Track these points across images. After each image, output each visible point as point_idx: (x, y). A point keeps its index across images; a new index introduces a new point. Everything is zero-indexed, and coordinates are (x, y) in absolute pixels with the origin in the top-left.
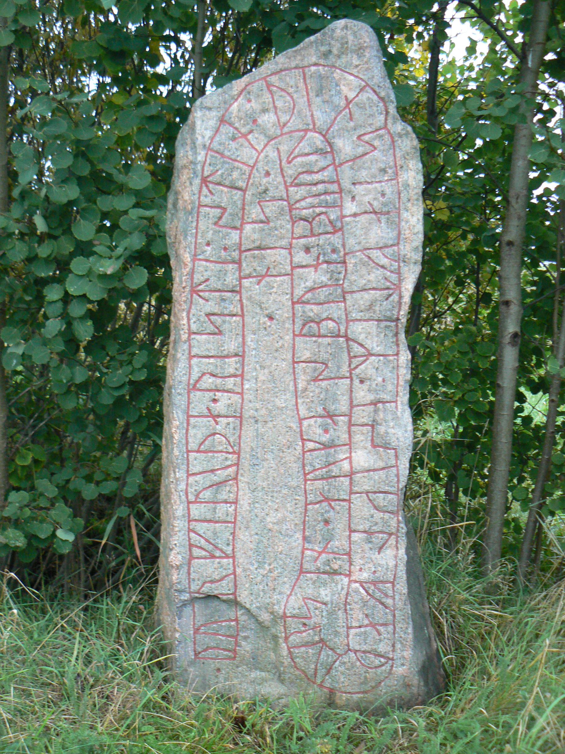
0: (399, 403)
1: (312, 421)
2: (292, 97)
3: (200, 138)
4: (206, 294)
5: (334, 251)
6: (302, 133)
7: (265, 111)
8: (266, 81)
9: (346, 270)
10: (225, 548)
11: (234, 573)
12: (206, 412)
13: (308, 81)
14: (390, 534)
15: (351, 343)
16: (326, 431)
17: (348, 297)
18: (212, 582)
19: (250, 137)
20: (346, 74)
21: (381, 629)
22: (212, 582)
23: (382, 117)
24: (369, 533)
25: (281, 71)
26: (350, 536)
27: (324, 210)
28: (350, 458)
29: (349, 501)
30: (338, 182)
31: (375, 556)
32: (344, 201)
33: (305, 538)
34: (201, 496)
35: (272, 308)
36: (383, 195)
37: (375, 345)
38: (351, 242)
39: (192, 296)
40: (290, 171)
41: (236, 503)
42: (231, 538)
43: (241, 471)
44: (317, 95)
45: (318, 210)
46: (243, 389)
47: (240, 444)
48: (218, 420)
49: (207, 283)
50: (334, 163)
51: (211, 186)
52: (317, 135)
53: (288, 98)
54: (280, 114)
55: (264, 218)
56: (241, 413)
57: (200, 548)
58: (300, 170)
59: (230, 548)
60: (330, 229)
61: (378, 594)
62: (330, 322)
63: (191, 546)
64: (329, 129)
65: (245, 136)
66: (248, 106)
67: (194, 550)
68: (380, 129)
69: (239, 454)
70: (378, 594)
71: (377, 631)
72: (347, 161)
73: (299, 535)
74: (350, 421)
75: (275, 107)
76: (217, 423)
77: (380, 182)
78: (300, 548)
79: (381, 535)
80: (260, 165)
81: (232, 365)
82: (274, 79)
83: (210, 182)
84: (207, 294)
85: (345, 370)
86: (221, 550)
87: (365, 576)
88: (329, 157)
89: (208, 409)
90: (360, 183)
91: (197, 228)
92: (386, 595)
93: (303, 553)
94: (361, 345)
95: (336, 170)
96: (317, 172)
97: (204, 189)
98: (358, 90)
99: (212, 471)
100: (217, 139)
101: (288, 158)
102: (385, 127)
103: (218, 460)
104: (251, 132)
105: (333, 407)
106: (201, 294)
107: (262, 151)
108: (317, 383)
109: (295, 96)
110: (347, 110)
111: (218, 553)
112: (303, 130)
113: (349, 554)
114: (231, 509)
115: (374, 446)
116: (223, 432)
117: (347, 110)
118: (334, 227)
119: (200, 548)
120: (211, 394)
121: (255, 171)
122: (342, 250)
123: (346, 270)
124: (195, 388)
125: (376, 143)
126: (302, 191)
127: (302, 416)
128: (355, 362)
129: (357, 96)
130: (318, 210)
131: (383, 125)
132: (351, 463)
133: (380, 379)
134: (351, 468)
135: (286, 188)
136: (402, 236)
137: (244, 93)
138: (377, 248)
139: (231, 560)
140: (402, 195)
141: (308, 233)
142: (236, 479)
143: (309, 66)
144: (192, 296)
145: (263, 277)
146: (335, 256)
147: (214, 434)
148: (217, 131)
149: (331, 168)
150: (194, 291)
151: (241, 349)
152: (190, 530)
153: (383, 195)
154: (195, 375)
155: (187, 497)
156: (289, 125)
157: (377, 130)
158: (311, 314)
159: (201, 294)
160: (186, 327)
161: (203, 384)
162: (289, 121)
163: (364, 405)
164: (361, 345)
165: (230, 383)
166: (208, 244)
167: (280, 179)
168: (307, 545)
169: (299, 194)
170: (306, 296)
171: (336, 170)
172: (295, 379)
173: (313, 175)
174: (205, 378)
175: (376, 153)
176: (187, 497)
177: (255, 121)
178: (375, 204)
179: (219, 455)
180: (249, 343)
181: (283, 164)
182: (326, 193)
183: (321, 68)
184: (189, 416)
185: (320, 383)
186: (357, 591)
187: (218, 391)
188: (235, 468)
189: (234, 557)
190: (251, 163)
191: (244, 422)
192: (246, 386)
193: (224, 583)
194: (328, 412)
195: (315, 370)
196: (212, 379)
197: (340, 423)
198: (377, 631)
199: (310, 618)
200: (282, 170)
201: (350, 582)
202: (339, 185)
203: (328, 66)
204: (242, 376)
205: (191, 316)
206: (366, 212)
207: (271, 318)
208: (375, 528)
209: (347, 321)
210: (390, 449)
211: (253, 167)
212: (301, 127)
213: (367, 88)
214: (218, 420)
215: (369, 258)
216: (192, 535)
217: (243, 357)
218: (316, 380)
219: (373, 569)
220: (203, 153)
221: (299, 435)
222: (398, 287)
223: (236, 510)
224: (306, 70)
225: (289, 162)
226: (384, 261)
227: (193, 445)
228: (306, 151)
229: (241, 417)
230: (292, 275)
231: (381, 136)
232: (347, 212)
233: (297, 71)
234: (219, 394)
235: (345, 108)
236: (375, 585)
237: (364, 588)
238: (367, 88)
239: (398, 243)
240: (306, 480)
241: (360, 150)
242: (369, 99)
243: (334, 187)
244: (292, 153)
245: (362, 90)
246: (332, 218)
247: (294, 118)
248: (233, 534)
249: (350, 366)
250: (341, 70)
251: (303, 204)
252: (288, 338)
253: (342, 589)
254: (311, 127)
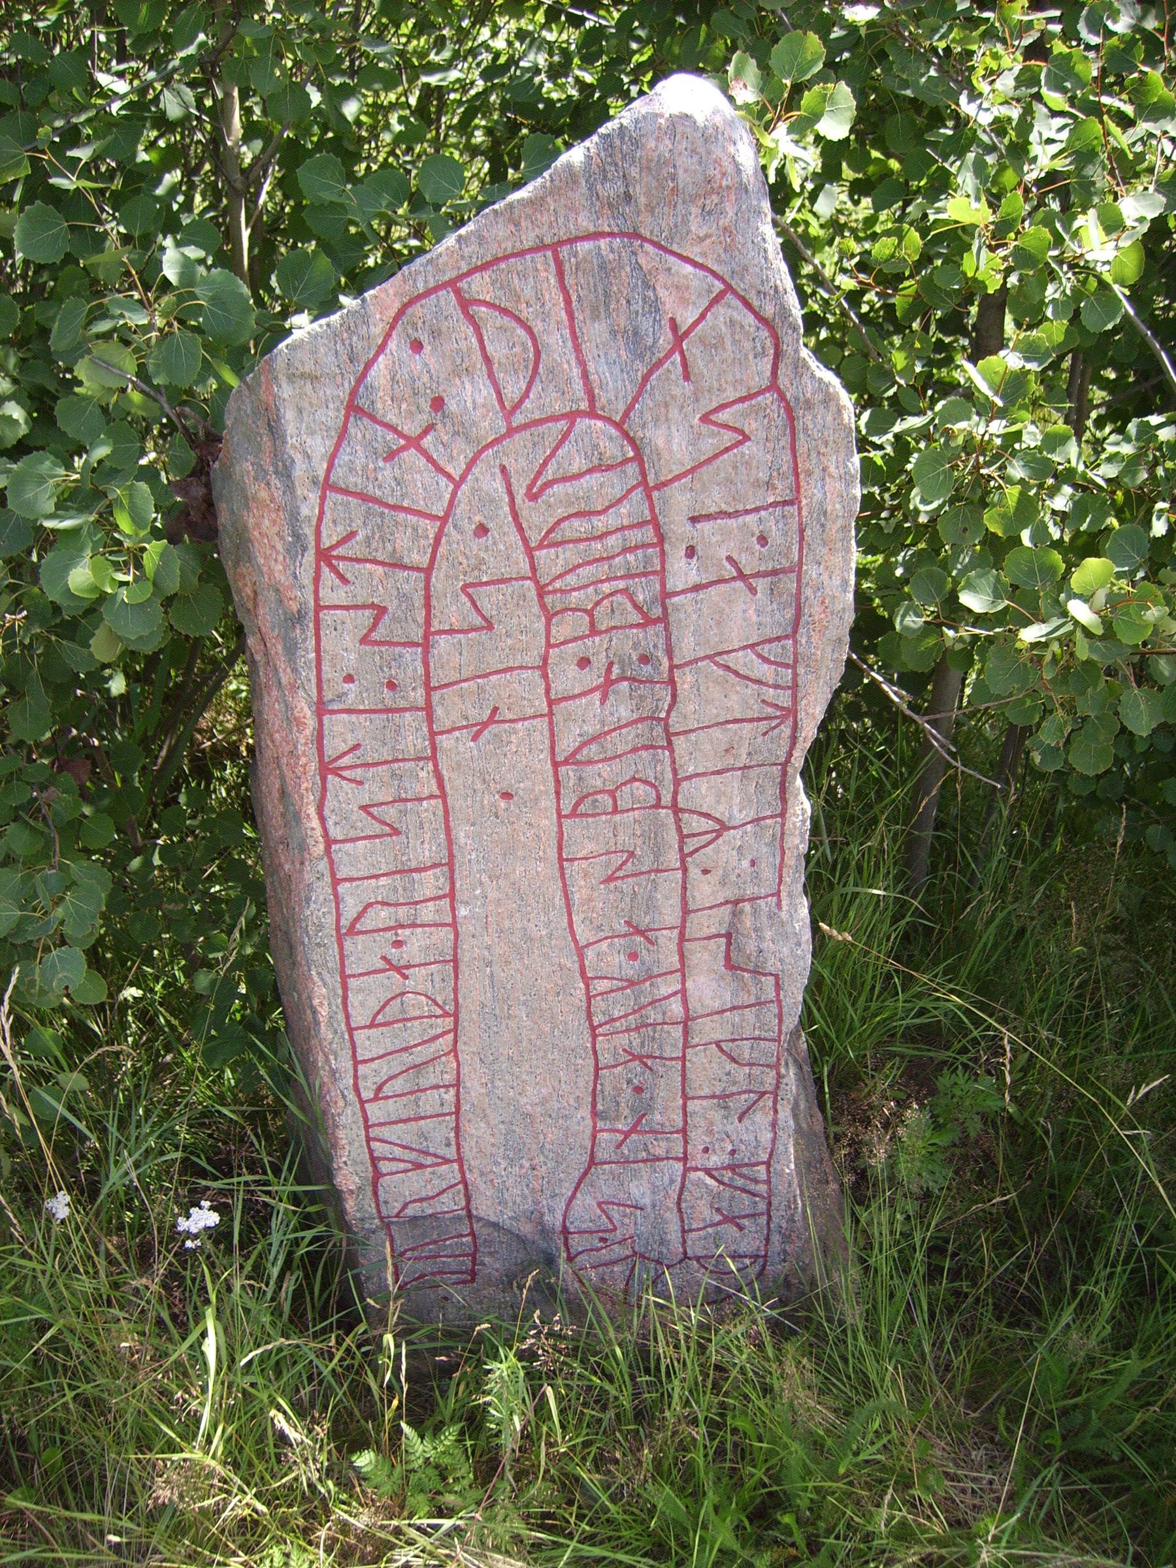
0: (783, 894)
1: (604, 946)
2: (529, 330)
3: (298, 458)
4: (358, 773)
5: (645, 659)
6: (563, 425)
7: (460, 371)
8: (458, 292)
9: (674, 696)
10: (440, 1152)
11: (464, 1181)
12: (381, 964)
13: (569, 281)
16: (633, 956)
17: (678, 742)
18: (421, 1200)
19: (428, 442)
20: (672, 259)
21: (745, 1222)
22: (421, 1200)
23: (766, 365)
24: (723, 1098)
25: (497, 260)
26: (684, 1106)
27: (621, 584)
28: (683, 992)
30: (655, 522)
31: (734, 1126)
32: (670, 560)
33: (595, 1114)
34: (385, 1089)
35: (509, 780)
36: (763, 540)
38: (687, 647)
39: (324, 780)
40: (537, 518)
41: (457, 1084)
42: (452, 1134)
44: (595, 317)
45: (606, 588)
46: (454, 916)
47: (456, 1000)
48: (406, 972)
49: (357, 752)
50: (644, 482)
52: (600, 424)
53: (520, 332)
55: (478, 621)
56: (455, 954)
58: (561, 512)
59: (454, 1148)
60: (636, 618)
61: (740, 1182)
62: (637, 784)
63: (374, 1160)
64: (630, 408)
65: (414, 442)
66: (416, 364)
68: (760, 393)
70: (740, 1182)
72: (678, 478)
73: (585, 1112)
75: (487, 360)
76: (406, 977)
77: (757, 510)
78: (588, 1132)
80: (461, 509)
82: (479, 286)
83: (339, 558)
84: (359, 771)
85: (672, 858)
86: (436, 1156)
87: (714, 1160)
89: (384, 958)
90: (709, 517)
92: (756, 1181)
93: (594, 1137)
94: (707, 816)
95: (649, 498)
99: (405, 1049)
100: (343, 457)
101: (530, 487)
102: (774, 386)
103: (415, 1032)
104: (429, 428)
106: (345, 773)
107: (463, 478)
108: (612, 885)
109: (538, 326)
110: (677, 357)
111: (429, 1160)
112: (563, 416)
113: (684, 1131)
115: (730, 965)
116: (420, 988)
118: (644, 615)
120: (389, 934)
121: (450, 528)
123: (674, 696)
124: (352, 931)
125: (751, 426)
129: (703, 316)
130: (606, 588)
131: (766, 383)
132: (685, 1002)
133: (745, 864)
135: (529, 551)
136: (804, 619)
137: (399, 327)
138: (744, 648)
139: (456, 1166)
140: (808, 532)
142: (455, 1050)
144: (324, 780)
145: (485, 725)
146: (647, 670)
147: (404, 994)
148: (343, 434)
149: (638, 495)
150: (327, 769)
151: (445, 852)
152: (369, 1139)
153: (763, 540)
154: (351, 909)
156: (527, 404)
157: (750, 397)
159: (345, 773)
160: (319, 831)
162: (526, 395)
163: (711, 908)
164: (707, 816)
166: (349, 679)
167: (514, 537)
168: (600, 1125)
169: (560, 562)
170: (585, 751)
171: (649, 498)
172: (565, 885)
173: (595, 520)
174: (371, 912)
175: (745, 448)
177: (438, 403)
178: (743, 560)
179: (416, 1023)
180: (462, 841)
182: (626, 550)
183: (603, 243)
184: (344, 978)
186: (699, 1183)
187: (402, 926)
189: (460, 1160)
191: (463, 967)
192: (463, 911)
193: (444, 1198)
195: (608, 864)
196: (384, 913)
199: (615, 1229)
201: (687, 1170)
202: (657, 527)
203: (622, 234)
204: (452, 895)
205: (326, 812)
207: (507, 796)
208: (734, 1089)
209: (677, 782)
210: (765, 975)
211: (444, 520)
212: (559, 407)
213: (729, 296)
214: (406, 972)
215: (727, 668)
217: (451, 864)
218: (610, 879)
219: (730, 1148)
220: (314, 497)
221: (577, 974)
222: (791, 713)
224: (564, 251)
225: (533, 497)
228: (575, 469)
229: (455, 961)
230: (551, 714)
231: (758, 411)
232: (675, 582)
233: (539, 257)
235: (668, 355)
237: (713, 1177)
238: (729, 296)
239: (795, 632)
240: (594, 1037)
241: (709, 445)
242: (732, 323)
243: (648, 534)
244: (539, 474)
247: (537, 387)
249: (681, 849)
251: (571, 580)
252: (548, 823)
253: (672, 1181)
254: (584, 406)
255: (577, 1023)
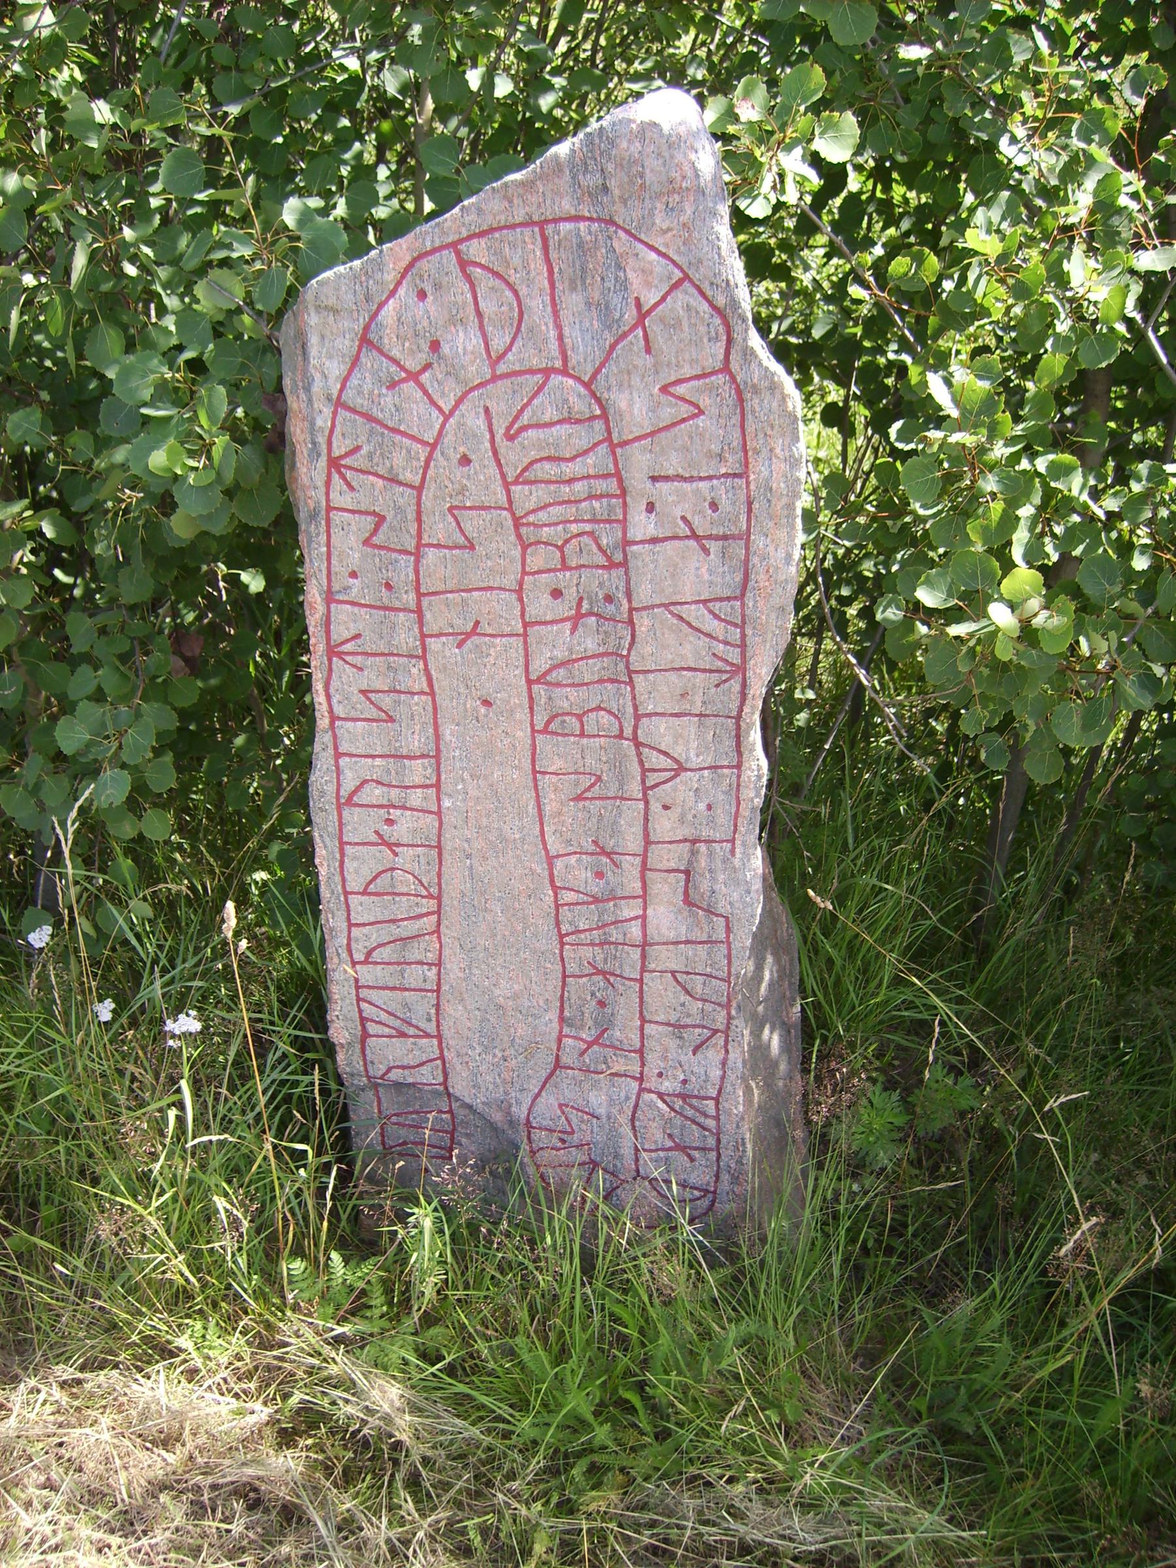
0: (738, 843)
1: (573, 860)
2: (516, 293)
3: (317, 376)
4: (358, 660)
5: (609, 599)
6: (539, 378)
7: (456, 321)
8: (458, 253)
9: (633, 636)
10: (422, 1025)
11: (442, 1058)
12: (374, 838)
13: (553, 255)
14: (716, 1031)
15: (646, 751)
16: (600, 875)
17: (638, 679)
18: (403, 1067)
19: (425, 378)
20: (640, 246)
21: (696, 1154)
22: (403, 1067)
23: (719, 349)
24: (678, 1027)
25: (492, 230)
26: (642, 1029)
27: (588, 527)
28: (644, 917)
29: (641, 981)
30: (618, 475)
31: (687, 1057)
32: (630, 511)
33: (562, 1019)
34: (374, 954)
35: (488, 689)
36: (714, 506)
37: (692, 754)
38: (644, 593)
39: (330, 661)
40: (514, 457)
41: (439, 964)
42: (433, 1011)
43: (444, 922)
44: (573, 289)
45: (574, 528)
46: (439, 806)
47: (440, 885)
48: (397, 849)
49: (359, 641)
50: (609, 439)
51: (349, 474)
52: (571, 382)
53: (508, 294)
54: (489, 329)
55: (462, 541)
56: (439, 841)
57: (380, 1023)
58: (534, 454)
59: (434, 1023)
60: (601, 560)
61: (690, 1112)
62: (602, 713)
63: (363, 1020)
64: (597, 371)
65: (414, 377)
66: (419, 310)
67: (368, 1024)
68: (714, 373)
69: (439, 898)
70: (690, 1112)
71: (689, 1156)
72: (639, 439)
73: (553, 1015)
74: (644, 863)
75: (479, 314)
76: (396, 854)
77: (710, 478)
78: (555, 1035)
79: (700, 1030)
80: (448, 439)
81: (419, 771)
82: (476, 250)
83: (346, 467)
84: (359, 658)
85: (635, 789)
86: (417, 1028)
87: (667, 1086)
88: (599, 425)
89: (377, 832)
90: (667, 478)
91: (328, 545)
92: (706, 1116)
93: (559, 1041)
94: (666, 754)
95: (614, 453)
96: (573, 459)
97: (335, 477)
98: (665, 288)
99: (393, 921)
100: (354, 381)
101: (508, 429)
102: (726, 368)
103: (403, 907)
104: (427, 366)
105: (612, 843)
106: (348, 658)
107: (452, 412)
108: (581, 804)
109: (523, 291)
110: (639, 332)
111: (412, 1031)
112: (539, 371)
113: (641, 1052)
114: (432, 974)
115: (687, 901)
116: (407, 867)
117: (639, 332)
118: (609, 558)
119: (380, 1023)
120: (382, 811)
121: (437, 454)
122: (625, 602)
123: (633, 636)
124: (349, 801)
125: (705, 401)
126: (539, 494)
127: (553, 853)
128: (652, 779)
129: (663, 299)
130: (574, 528)
131: (719, 365)
132: (644, 926)
133: (702, 806)
134: (645, 935)
135: (506, 485)
136: (751, 584)
137: (409, 277)
138: (697, 602)
139: (435, 1042)
140: (756, 506)
141: (556, 562)
142: (438, 931)
143: (556, 221)
144: (330, 661)
145: (468, 635)
146: (610, 609)
147: (393, 869)
148: (355, 361)
149: (603, 449)
150: (333, 652)
151: (432, 745)
152: (359, 999)
153: (714, 506)
154: (349, 784)
155: (351, 955)
156: (510, 356)
157: (704, 376)
158: (566, 705)
159: (348, 658)
160: (325, 707)
161: (363, 797)
162: (509, 348)
163: (671, 842)
164: (666, 754)
165: (416, 798)
166: (354, 575)
167: (493, 470)
168: (566, 1030)
169: (534, 499)
170: (554, 674)
171: (614, 453)
172: (538, 796)
173: (563, 465)
174: (367, 788)
175: (701, 421)
176: (351, 955)
177: (435, 346)
178: (696, 521)
179: (404, 899)
180: (448, 738)
181: (498, 439)
182: (591, 497)
183: (582, 226)
184: (342, 844)
185: (587, 803)
186: (652, 1105)
187: (394, 807)
188: (434, 918)
189: (439, 1037)
190: (429, 437)
191: (446, 855)
192: (446, 803)
193: (424, 1070)
194: (602, 848)
195: (577, 783)
196: (378, 791)
197: (625, 865)
198: (689, 1156)
199: (573, 1132)
200: (495, 453)
201: (641, 1090)
202: (620, 481)
203: (599, 220)
204: (437, 785)
205: (332, 691)
206: (675, 537)
207: (487, 703)
208: (689, 1021)
209: (638, 717)
210: (717, 915)
211: (433, 446)
212: (535, 363)
213: (686, 284)
214: (397, 849)
215: (681, 618)
216: (364, 1005)
217: (437, 757)
218: (579, 798)
219: (682, 1077)
220: (327, 411)
221: (547, 881)
222: (740, 669)
223: (439, 974)
224: (549, 229)
225: (511, 438)
226: (712, 625)
227: (354, 884)
228: (546, 418)
229: (439, 847)
230: (525, 635)
231: (711, 389)
232: (635, 533)
233: (527, 232)
234: (395, 813)
235: (633, 328)
236: (684, 1100)
237: (665, 1102)
238: (686, 284)
239: (743, 595)
240: (562, 944)
241: (670, 411)
242: (688, 308)
243: (612, 486)
244: (516, 418)
245: (675, 286)
246: (604, 542)
247: (519, 342)
248: (438, 1006)
249: (643, 782)
250: (628, 232)
251: (542, 516)
252: (522, 735)
253: (627, 1098)
254: (558, 364)
255: (546, 926)
